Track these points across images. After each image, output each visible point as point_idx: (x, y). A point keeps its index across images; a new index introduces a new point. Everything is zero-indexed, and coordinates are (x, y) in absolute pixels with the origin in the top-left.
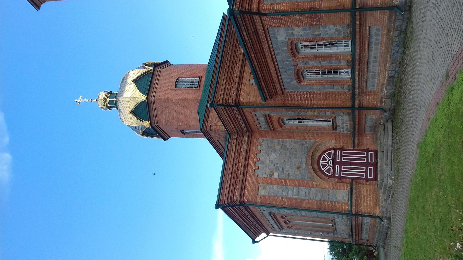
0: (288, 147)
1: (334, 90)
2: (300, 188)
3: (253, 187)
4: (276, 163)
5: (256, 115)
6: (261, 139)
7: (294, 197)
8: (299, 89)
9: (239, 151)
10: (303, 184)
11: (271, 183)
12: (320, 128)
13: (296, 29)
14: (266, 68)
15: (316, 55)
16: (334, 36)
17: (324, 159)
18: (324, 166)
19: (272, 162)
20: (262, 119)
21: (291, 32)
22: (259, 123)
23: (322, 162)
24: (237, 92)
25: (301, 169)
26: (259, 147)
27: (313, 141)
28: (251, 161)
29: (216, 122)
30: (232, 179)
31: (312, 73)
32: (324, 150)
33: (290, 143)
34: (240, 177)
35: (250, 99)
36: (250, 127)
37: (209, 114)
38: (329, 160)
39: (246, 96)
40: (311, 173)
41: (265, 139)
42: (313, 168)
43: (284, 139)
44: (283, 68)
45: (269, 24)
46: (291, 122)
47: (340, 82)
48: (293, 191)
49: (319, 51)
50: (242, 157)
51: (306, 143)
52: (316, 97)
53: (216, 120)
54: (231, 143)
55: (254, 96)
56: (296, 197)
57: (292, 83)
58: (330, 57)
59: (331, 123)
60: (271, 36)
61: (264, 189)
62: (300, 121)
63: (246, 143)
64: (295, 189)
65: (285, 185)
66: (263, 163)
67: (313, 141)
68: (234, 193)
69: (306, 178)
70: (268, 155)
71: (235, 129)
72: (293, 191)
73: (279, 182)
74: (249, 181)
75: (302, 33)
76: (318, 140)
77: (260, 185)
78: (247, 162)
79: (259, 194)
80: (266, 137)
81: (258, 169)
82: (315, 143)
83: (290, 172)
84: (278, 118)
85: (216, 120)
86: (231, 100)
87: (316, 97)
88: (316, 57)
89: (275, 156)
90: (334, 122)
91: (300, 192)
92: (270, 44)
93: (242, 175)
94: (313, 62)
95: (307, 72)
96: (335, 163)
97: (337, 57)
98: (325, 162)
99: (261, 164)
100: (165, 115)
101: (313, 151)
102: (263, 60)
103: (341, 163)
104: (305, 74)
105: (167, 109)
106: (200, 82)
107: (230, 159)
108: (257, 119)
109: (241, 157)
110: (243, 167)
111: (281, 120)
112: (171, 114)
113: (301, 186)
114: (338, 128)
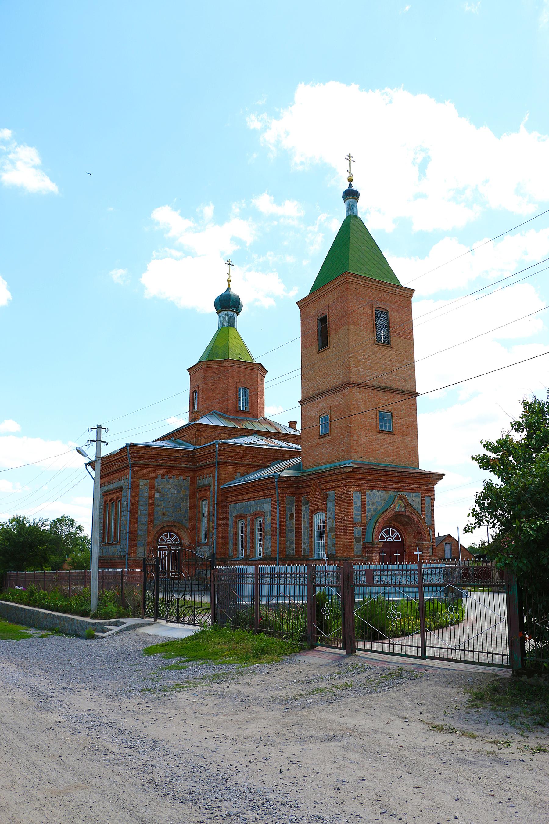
0: (182, 504)
1: (230, 544)
2: (147, 516)
5: (210, 477)
6: (188, 479)
7: (139, 511)
8: (231, 516)
10: (151, 519)
11: (150, 490)
12: (199, 532)
13: (270, 519)
17: (172, 536)
18: (166, 536)
19: (169, 490)
20: (206, 482)
24: (229, 463)
25: (163, 516)
26: (182, 478)
27: (188, 526)
28: (168, 471)
29: (204, 435)
33: (185, 505)
34: (155, 462)
40: (160, 525)
42: (164, 527)
46: (204, 507)
47: (235, 549)
48: (144, 510)
54: (185, 453)
56: (139, 513)
57: (235, 511)
58: (253, 542)
59: (203, 541)
62: (205, 515)
63: (185, 466)
64: (146, 512)
65: (149, 503)
66: (168, 482)
68: (140, 458)
70: (175, 487)
71: (197, 456)
72: (144, 510)
73: (151, 497)
74: (151, 471)
80: (190, 484)
81: (162, 478)
82: (186, 527)
83: (160, 507)
88: (252, 533)
90: (204, 545)
91: (143, 517)
93: (157, 464)
97: (253, 547)
98: (169, 537)
108: (206, 478)
113: (149, 517)
114: (200, 547)
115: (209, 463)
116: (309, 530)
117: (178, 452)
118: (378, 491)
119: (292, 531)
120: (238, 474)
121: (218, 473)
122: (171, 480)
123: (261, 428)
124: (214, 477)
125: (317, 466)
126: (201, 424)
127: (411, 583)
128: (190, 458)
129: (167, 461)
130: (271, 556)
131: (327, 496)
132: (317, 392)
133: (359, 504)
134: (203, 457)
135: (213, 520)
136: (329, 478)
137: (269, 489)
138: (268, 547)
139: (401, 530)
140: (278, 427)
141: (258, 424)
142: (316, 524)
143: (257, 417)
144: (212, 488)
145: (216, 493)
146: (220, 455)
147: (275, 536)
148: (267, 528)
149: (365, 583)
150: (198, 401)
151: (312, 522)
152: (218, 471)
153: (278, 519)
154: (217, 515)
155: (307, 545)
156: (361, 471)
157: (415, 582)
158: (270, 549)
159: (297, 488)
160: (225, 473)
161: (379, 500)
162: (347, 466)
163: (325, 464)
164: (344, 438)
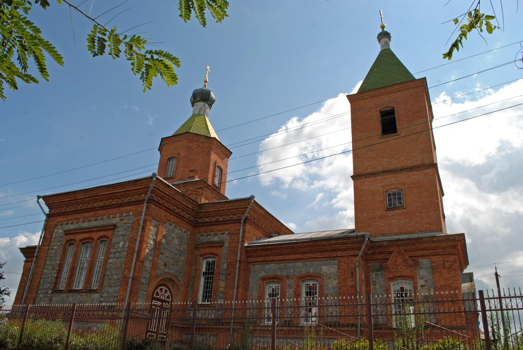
6: (189, 233)
9: (185, 210)
10: (155, 266)
13: (335, 282)
15: (300, 296)
21: (332, 277)
26: (184, 230)
29: (204, 194)
37: (210, 190)
53: (205, 195)
54: (193, 205)
69: (158, 271)
74: (163, 213)
78: (177, 215)
81: (170, 225)
84: (217, 253)
85: (205, 195)
89: (176, 244)
122: (176, 229)
128: (195, 211)
134: (213, 213)
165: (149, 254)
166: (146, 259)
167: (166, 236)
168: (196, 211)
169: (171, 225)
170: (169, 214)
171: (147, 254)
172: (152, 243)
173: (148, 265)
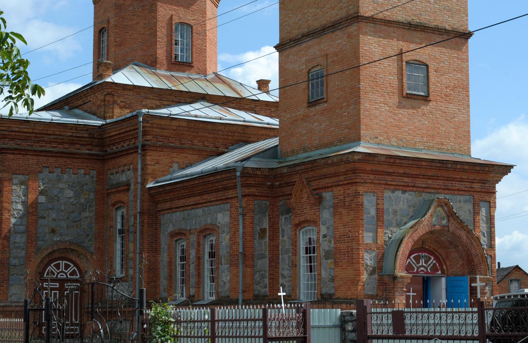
0: (84, 215)
3: (24, 166)
4: (59, 198)
5: (129, 170)
6: (94, 173)
12: (112, 259)
13: (228, 237)
14: (188, 194)
16: (220, 281)
17: (67, 267)
18: (58, 266)
19: (62, 190)
20: (123, 178)
21: (225, 231)
22: (117, 173)
23: (62, 263)
25: (52, 235)
26: (82, 171)
27: (92, 249)
28: (61, 161)
29: (119, 102)
30: (34, 135)
31: (183, 251)
32: (81, 266)
34: (37, 147)
35: (151, 165)
36: (111, 158)
38: (66, 274)
39: (155, 159)
41: (95, 179)
43: (94, 208)
44: (189, 215)
45: (233, 205)
46: (119, 219)
49: (206, 262)
50: (66, 147)
51: (89, 241)
52: (153, 256)
53: (121, 102)
54: (87, 130)
55: (154, 170)
60: (222, 205)
61: (21, 182)
62: (121, 232)
63: (88, 152)
67: (92, 249)
69: (39, 243)
70: (71, 187)
71: (108, 135)
72: (20, 225)
74: (32, 161)
75: (224, 244)
76: (95, 257)
77: (27, 177)
78: (60, 155)
79: (14, 176)
81: (50, 172)
85: (121, 102)
86: (149, 139)
87: (153, 256)
88: (199, 259)
89: (69, 196)
91: (19, 235)
92: (214, 203)
93: (40, 149)
94: (194, 255)
95: (183, 245)
96: (62, 282)
97: (199, 283)
98: (62, 267)
99: (57, 175)
100: (131, 4)
101: (78, 251)
102: (196, 192)
103: (61, 289)
104: (181, 242)
105: (140, 10)
106: (185, 64)
107: (63, 130)
108: (123, 171)
109: (66, 146)
110: (51, 149)
111: (122, 205)
112: (133, 15)
115: (127, 148)
116: (290, 254)
117: (76, 130)
118: (404, 192)
119: (263, 257)
120: (175, 166)
121: (142, 164)
122: (65, 176)
123: (211, 90)
124: (135, 170)
125: (305, 151)
126: (113, 83)
127: (466, 333)
128: (96, 138)
129: (59, 143)
130: (228, 297)
131: (320, 200)
132: (305, 31)
133: (373, 212)
134: (117, 137)
135: (135, 239)
136: (325, 171)
137: (226, 189)
138: (225, 283)
139: (441, 255)
140: (239, 88)
141: (208, 84)
142: (302, 245)
143: (204, 72)
144: (132, 187)
145: (139, 196)
146: (145, 133)
147: (237, 265)
148: (223, 252)
149: (391, 334)
150: (108, 45)
151: (296, 242)
152: (143, 161)
153: (241, 236)
154: (142, 232)
155: (287, 279)
156: (376, 159)
157: (473, 332)
158: (228, 285)
159: (272, 187)
160: (153, 163)
161: (406, 207)
162: (353, 152)
163: (317, 148)
164: (348, 106)
165: (18, 224)
166: (12, 232)
167: (46, 191)
168: (98, 137)
169: (53, 173)
170: (44, 159)
171: (14, 225)
172: (20, 207)
173: (20, 239)
